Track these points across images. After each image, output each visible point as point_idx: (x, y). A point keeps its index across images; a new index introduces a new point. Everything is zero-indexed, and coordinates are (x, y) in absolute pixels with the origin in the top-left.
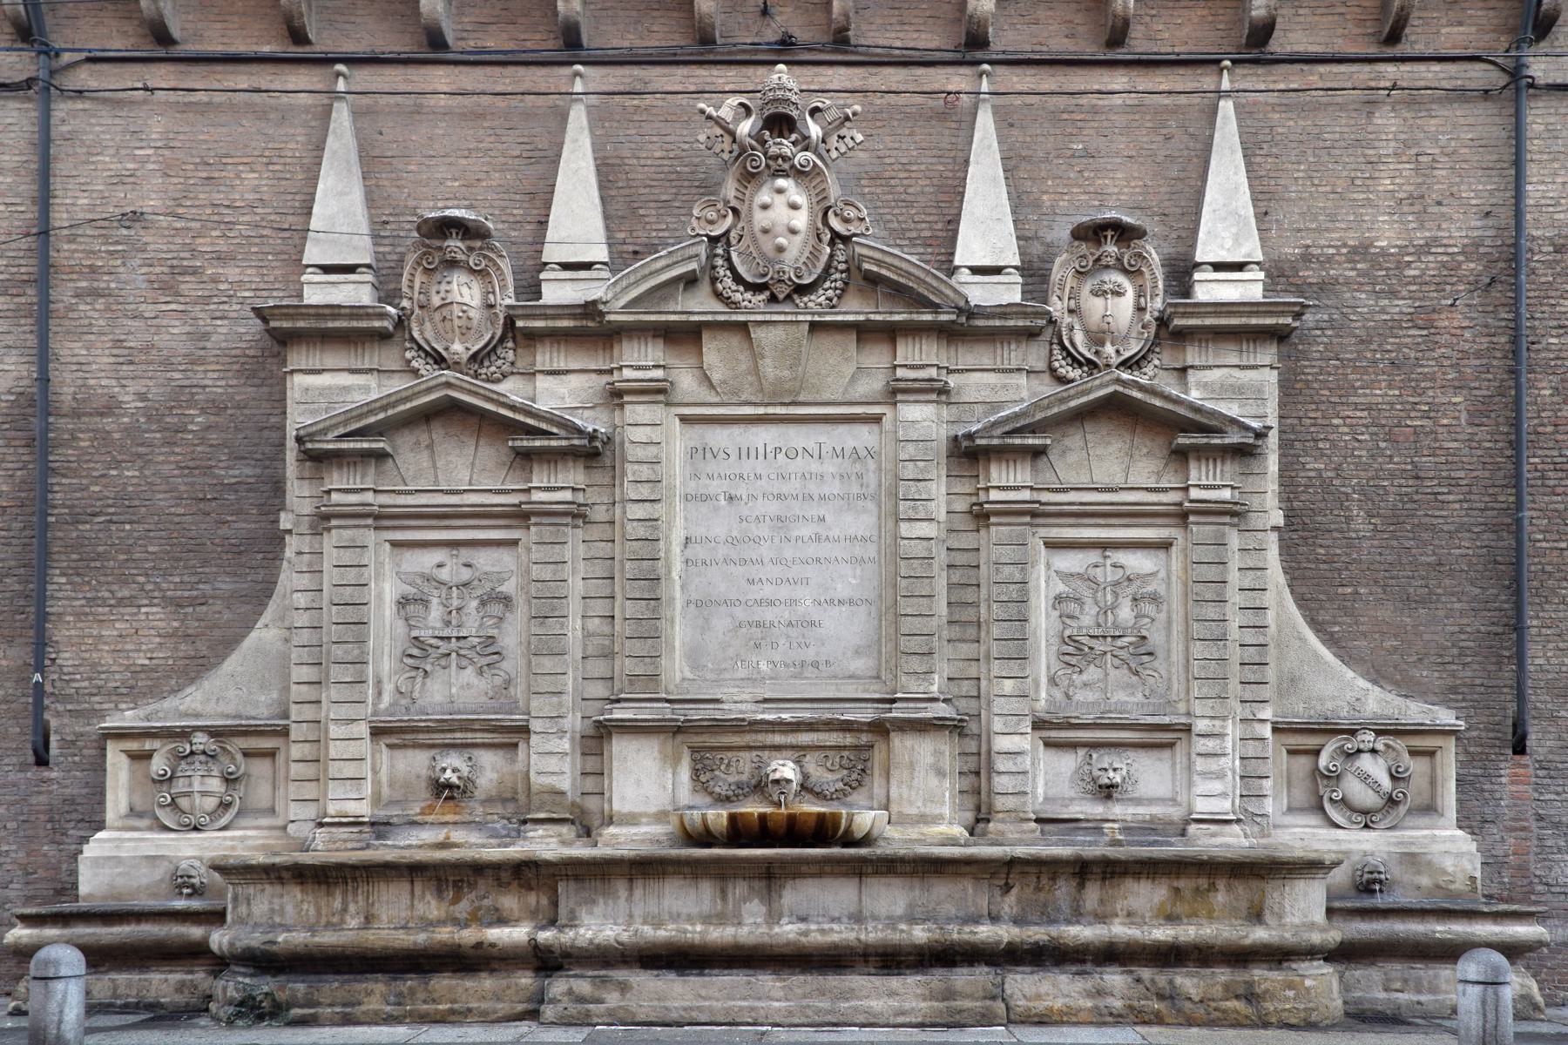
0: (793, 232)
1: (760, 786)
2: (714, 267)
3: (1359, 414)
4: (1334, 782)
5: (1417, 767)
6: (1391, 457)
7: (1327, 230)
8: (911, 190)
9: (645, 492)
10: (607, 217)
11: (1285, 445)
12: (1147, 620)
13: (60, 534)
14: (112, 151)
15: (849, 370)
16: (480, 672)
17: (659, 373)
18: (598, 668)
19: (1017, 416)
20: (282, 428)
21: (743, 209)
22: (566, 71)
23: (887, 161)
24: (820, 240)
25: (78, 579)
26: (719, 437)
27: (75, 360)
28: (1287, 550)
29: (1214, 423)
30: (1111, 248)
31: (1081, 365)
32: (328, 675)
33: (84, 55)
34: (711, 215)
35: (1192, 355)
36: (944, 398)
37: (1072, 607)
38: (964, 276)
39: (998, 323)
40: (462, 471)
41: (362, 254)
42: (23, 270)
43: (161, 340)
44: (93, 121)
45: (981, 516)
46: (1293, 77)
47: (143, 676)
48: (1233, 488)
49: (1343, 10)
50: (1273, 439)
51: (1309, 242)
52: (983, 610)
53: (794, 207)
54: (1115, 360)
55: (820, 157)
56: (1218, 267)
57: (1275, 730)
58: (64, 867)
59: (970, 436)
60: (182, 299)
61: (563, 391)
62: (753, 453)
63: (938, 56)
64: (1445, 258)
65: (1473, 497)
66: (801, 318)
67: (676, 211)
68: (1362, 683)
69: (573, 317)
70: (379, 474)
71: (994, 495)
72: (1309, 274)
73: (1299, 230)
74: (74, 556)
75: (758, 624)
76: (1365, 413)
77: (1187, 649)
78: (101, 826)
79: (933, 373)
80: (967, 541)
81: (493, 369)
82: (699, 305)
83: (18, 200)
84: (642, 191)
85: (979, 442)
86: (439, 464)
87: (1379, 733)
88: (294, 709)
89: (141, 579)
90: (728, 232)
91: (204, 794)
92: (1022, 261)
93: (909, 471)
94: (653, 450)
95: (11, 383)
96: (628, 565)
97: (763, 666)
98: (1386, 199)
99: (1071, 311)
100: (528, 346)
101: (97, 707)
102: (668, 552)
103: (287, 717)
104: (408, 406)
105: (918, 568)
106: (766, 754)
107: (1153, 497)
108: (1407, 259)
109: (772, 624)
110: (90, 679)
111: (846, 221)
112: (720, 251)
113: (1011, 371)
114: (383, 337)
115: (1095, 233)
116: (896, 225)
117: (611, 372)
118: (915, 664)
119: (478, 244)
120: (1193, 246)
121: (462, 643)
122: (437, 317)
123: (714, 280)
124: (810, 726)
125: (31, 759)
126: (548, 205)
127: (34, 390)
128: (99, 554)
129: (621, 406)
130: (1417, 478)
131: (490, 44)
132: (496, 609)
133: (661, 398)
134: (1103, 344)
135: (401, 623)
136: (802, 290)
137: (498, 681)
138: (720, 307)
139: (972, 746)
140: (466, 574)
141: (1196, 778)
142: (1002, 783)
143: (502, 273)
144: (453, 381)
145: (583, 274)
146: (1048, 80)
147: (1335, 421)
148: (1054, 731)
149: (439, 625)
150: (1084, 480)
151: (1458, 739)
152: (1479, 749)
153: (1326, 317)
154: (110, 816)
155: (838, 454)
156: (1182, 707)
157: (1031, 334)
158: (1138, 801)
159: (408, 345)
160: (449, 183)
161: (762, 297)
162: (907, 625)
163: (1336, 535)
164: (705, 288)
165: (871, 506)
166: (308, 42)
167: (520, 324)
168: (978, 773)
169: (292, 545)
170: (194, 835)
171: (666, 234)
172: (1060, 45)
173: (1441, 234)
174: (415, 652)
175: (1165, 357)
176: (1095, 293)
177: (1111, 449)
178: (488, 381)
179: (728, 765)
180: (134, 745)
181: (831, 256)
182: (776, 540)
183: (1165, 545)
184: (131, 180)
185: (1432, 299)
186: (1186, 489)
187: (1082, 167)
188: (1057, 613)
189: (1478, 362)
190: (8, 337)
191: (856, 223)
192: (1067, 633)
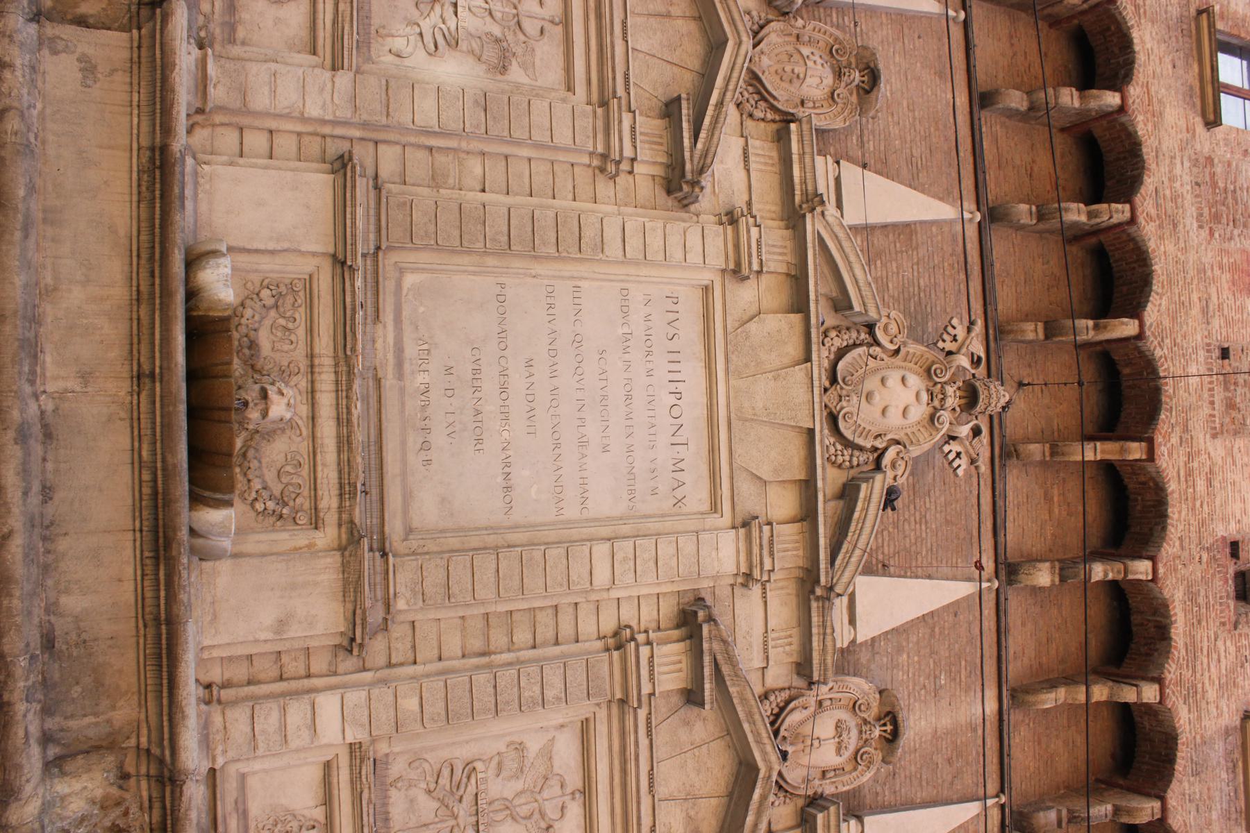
0: (884, 412)
8: (907, 527)
9: (634, 243)
17: (755, 267)
21: (897, 361)
22: (973, 207)
24: (876, 437)
26: (690, 329)
30: (877, 732)
34: (893, 328)
36: (740, 580)
37: (511, 765)
53: (905, 412)
59: (710, 619)
63: (1001, 539)
66: (817, 418)
71: (645, 651)
75: (476, 371)
79: (767, 566)
80: (588, 627)
84: (894, 265)
86: (652, 19)
90: (878, 344)
93: (666, 549)
94: (679, 255)
97: (421, 378)
99: (820, 703)
106: (304, 384)
109: (477, 389)
111: (893, 465)
113: (766, 651)
115: (888, 713)
118: (434, 576)
119: (854, 99)
122: (790, 48)
123: (837, 328)
124: (345, 443)
132: (491, 53)
133: (732, 266)
136: (833, 419)
137: (399, 43)
139: (319, 664)
140: (531, 27)
142: (268, 718)
162: (486, 564)
165: (621, 509)
167: (793, 126)
168: (281, 679)
176: (838, 726)
179: (286, 329)
181: (861, 449)
188: (503, 749)
192: (479, 766)
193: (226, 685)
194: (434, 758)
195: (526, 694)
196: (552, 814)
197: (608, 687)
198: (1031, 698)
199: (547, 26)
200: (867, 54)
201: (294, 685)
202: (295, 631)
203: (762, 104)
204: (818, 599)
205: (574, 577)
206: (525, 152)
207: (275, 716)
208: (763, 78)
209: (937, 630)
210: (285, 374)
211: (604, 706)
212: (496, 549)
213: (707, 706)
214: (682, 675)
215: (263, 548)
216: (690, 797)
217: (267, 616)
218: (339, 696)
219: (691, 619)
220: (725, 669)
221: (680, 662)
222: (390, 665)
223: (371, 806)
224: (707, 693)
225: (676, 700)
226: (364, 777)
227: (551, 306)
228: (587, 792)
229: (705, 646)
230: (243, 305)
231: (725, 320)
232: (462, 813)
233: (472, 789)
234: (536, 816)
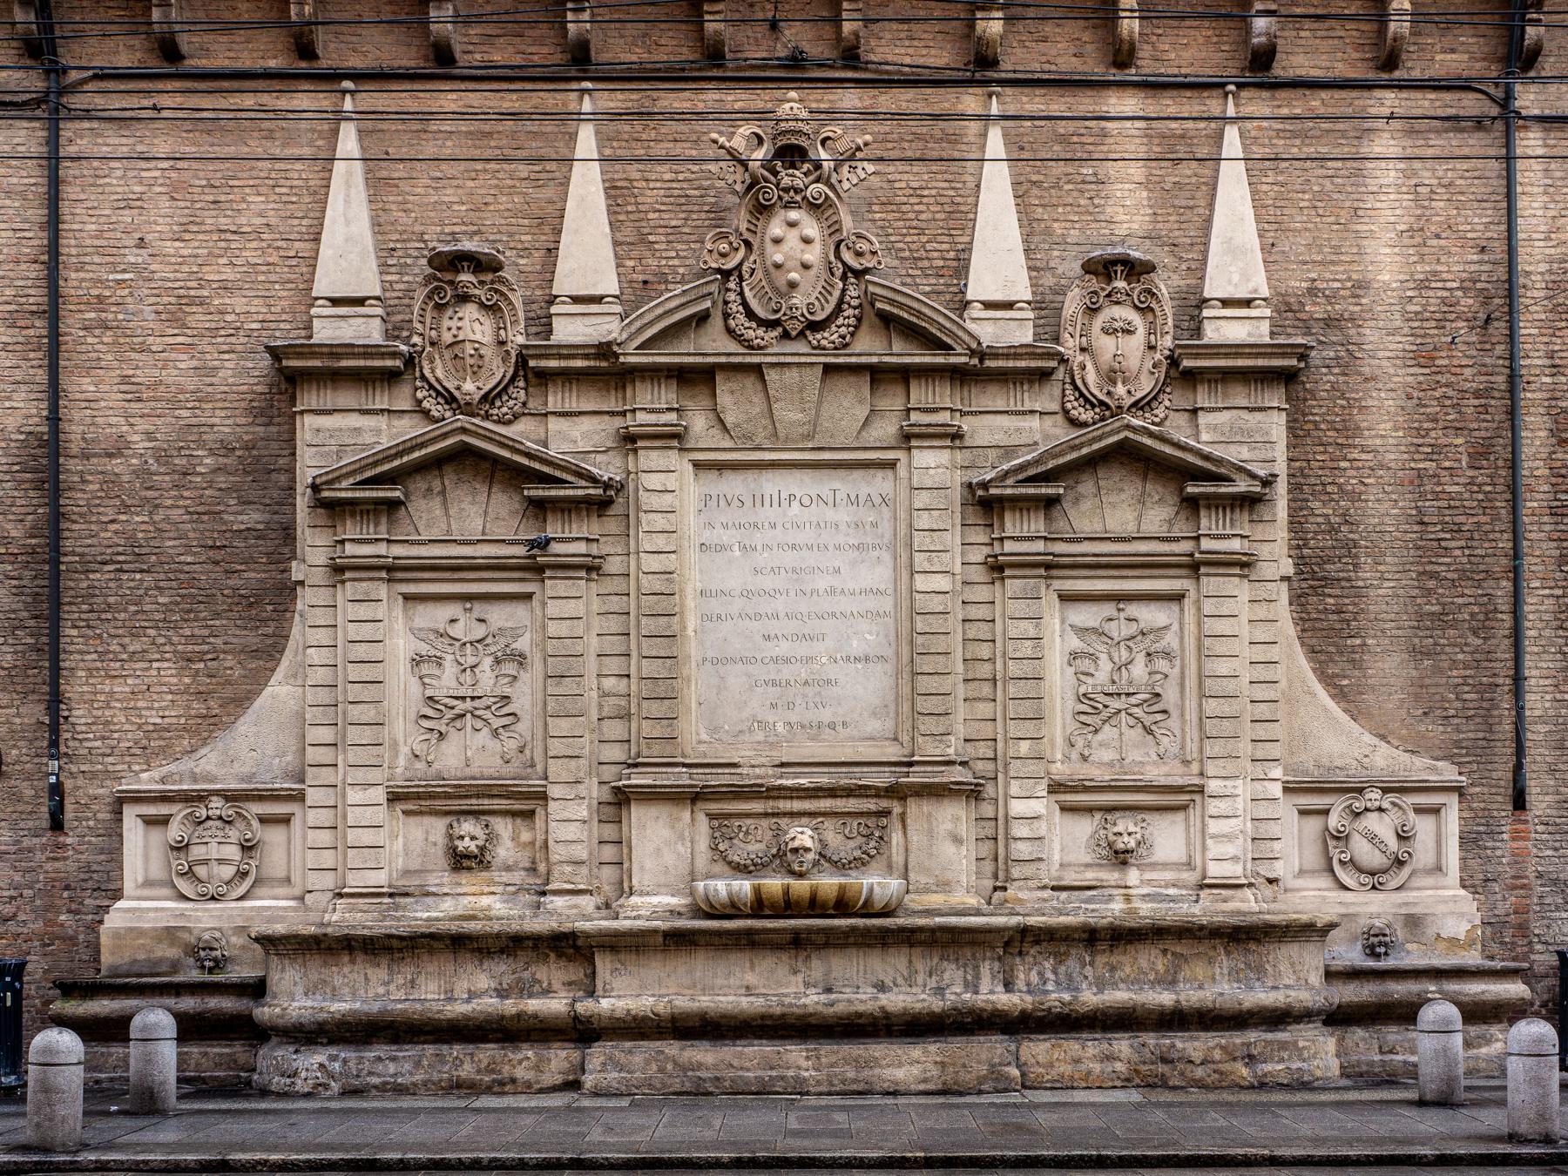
1: (783, 858)
2: (726, 303)
3: (1364, 456)
5: (1424, 827)
7: (1333, 263)
8: (923, 217)
9: (660, 542)
10: (616, 243)
11: (1295, 488)
12: (1159, 676)
13: (72, 584)
14: (119, 173)
15: (862, 412)
16: (495, 733)
17: (672, 417)
18: (615, 729)
19: (1028, 465)
20: (291, 471)
23: (897, 185)
25: (90, 632)
26: (734, 484)
27: (83, 396)
28: (1297, 599)
29: (1223, 470)
30: (1120, 284)
31: (1093, 406)
32: (344, 736)
33: (90, 73)
35: (1203, 398)
36: (957, 442)
37: (1085, 665)
38: (976, 311)
39: (1011, 364)
40: (473, 519)
41: (370, 285)
42: (31, 300)
43: (169, 376)
44: (100, 141)
45: (997, 569)
46: (1296, 103)
47: (155, 735)
48: (1242, 537)
49: (1342, 33)
50: (1281, 487)
51: (1313, 275)
52: (999, 665)
53: (807, 241)
54: (1128, 401)
55: (832, 187)
56: (1226, 303)
57: (1286, 790)
58: (81, 937)
59: (985, 485)
60: (189, 332)
61: (576, 434)
62: (767, 502)
64: (1446, 294)
65: (1475, 544)
67: (685, 237)
68: (1368, 738)
69: (586, 357)
70: (391, 522)
71: (1009, 547)
72: (1316, 310)
73: (1305, 263)
74: (85, 607)
76: (1369, 457)
77: (1200, 705)
78: (117, 895)
79: (944, 417)
81: (505, 410)
82: (713, 344)
83: (26, 226)
84: (651, 216)
85: (993, 491)
87: (1385, 791)
88: (310, 771)
89: (152, 632)
91: (221, 861)
92: (1034, 293)
93: (923, 521)
94: (668, 497)
95: (21, 421)
96: (644, 621)
97: (780, 728)
98: (1388, 231)
99: (1083, 350)
100: (540, 385)
101: (110, 768)
102: (682, 605)
103: (303, 781)
104: (423, 452)
105: (936, 624)
106: (783, 822)
108: (1409, 293)
110: (103, 738)
111: (859, 254)
112: (732, 285)
113: (1024, 413)
114: (390, 378)
115: (1105, 267)
116: (907, 254)
117: (623, 414)
119: (489, 277)
120: (1202, 278)
121: (477, 703)
122: (448, 355)
123: (726, 316)
124: (832, 792)
125: (46, 824)
126: (558, 232)
127: (45, 429)
128: (109, 605)
129: (635, 451)
130: (1422, 523)
131: (497, 57)
132: (509, 668)
134: (1115, 383)
135: (414, 683)
136: (815, 327)
137: (512, 745)
138: (733, 347)
139: (987, 810)
140: (479, 631)
141: (1209, 842)
143: (514, 308)
144: (468, 426)
145: (594, 308)
146: (1057, 103)
147: (1343, 464)
148: (1070, 795)
149: (454, 684)
151: (1461, 795)
152: (1482, 805)
153: (1332, 354)
154: (128, 886)
155: (854, 501)
156: (1195, 768)
157: (1044, 375)
158: (1154, 866)
159: (418, 384)
160: (456, 207)
161: (775, 333)
162: (924, 684)
164: (717, 321)
165: (887, 557)
166: (315, 57)
167: (532, 363)
168: (996, 839)
169: (305, 598)
170: (212, 905)
171: (676, 262)
172: (1066, 63)
173: (1439, 268)
174: (430, 713)
175: (1176, 398)
176: (1105, 331)
177: (1123, 496)
178: (499, 422)
180: (151, 810)
181: (844, 290)
182: (792, 594)
183: (1178, 597)
184: (139, 203)
185: (1432, 336)
186: (1197, 538)
187: (1092, 194)
188: (1072, 670)
189: (1476, 402)
190: (17, 371)
191: (868, 256)
192: (1082, 690)
193: (996, 877)
194: (1072, 726)
195: (1029, 653)
196: (1133, 629)
198: (1126, 47)
199: (475, 614)
200: (436, 262)
201: (1001, 831)
202: (963, 830)
203: (511, 389)
204: (981, 361)
205: (940, 609)
206: (595, 640)
207: (1021, 846)
208: (487, 388)
209: (1034, 178)
210: (778, 832)
212: (914, 674)
213: (1061, 491)
215: (902, 850)
217: (949, 849)
219: (986, 505)
220: (1032, 472)
222: (995, 759)
224: (1050, 491)
225: (1056, 512)
227: (719, 617)
229: (1009, 491)
230: (730, 863)
231: (724, 450)
233: (1101, 698)
234: (1130, 643)
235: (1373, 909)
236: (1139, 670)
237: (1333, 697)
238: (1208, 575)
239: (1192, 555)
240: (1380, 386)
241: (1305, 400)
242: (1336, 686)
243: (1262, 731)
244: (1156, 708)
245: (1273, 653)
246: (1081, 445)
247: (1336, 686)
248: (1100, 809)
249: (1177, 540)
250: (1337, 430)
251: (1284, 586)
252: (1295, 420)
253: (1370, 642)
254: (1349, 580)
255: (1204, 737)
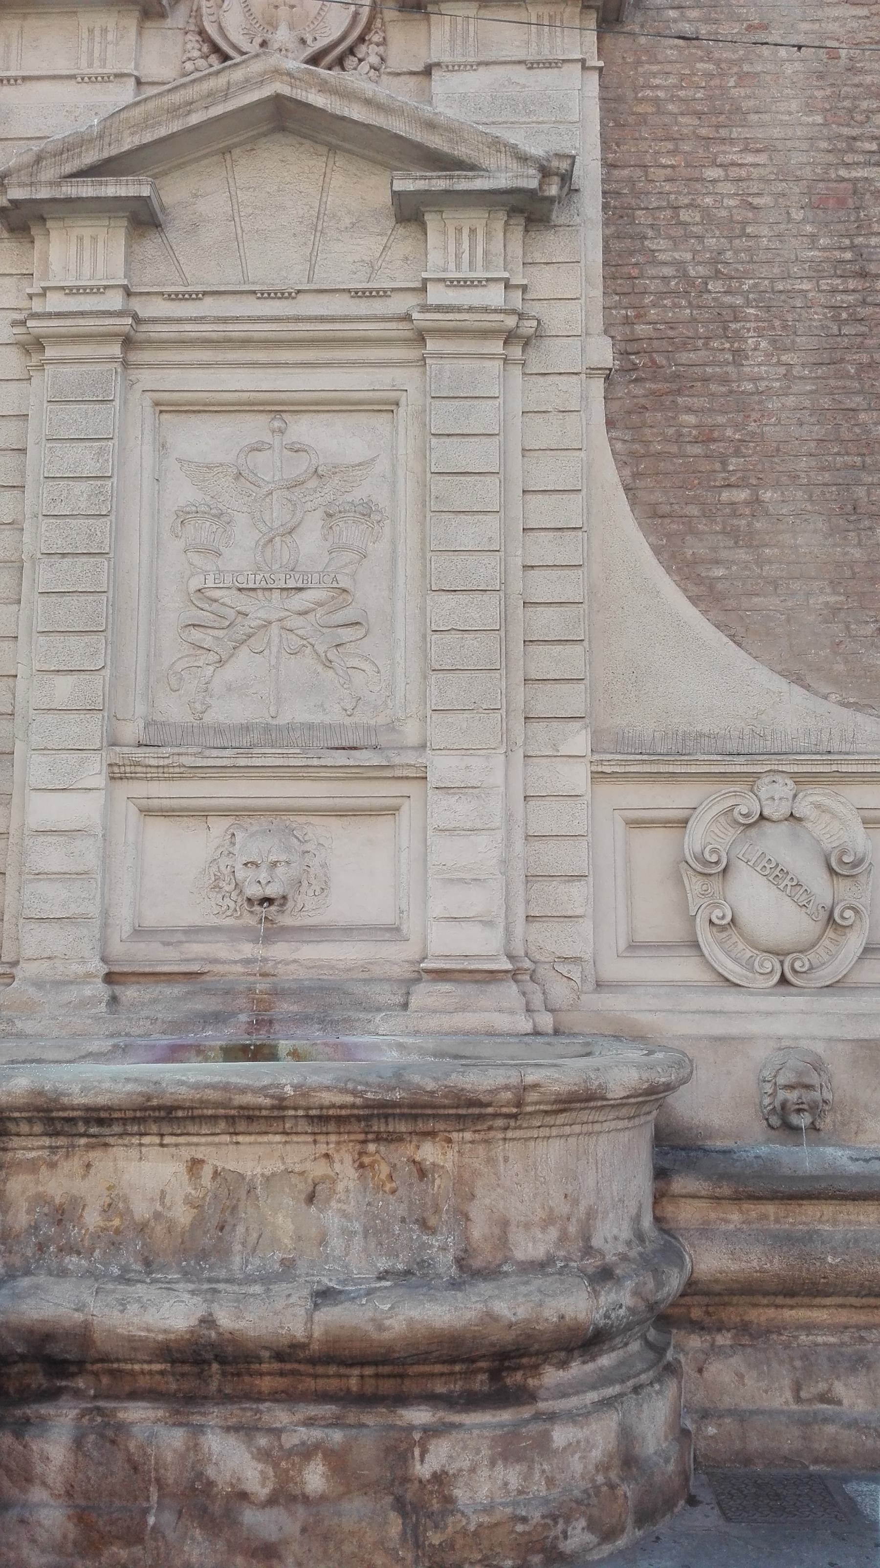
3: (750, 159)
4: (715, 885)
6: (813, 237)
68: (764, 678)
76: (762, 159)
77: (423, 610)
87: (802, 780)
107: (363, 307)
147: (712, 173)
150: (231, 278)
163: (713, 387)
192: (195, 583)
195: (83, 506)
196: (301, 466)
197: (98, 368)
207: (46, 889)
211: (134, 374)
214: (102, 233)
216: (317, 225)
218: (33, 793)
220: (90, 158)
221: (80, 239)
223: (207, 753)
225: (150, 246)
226: (161, 762)
228: (277, 408)
229: (44, 193)
232: (262, 614)
233: (228, 597)
235: (783, 1027)
236: (310, 542)
237: (694, 600)
238: (441, 356)
239: (407, 318)
240: (775, 37)
241: (639, 63)
242: (699, 580)
243: (546, 661)
244: (340, 617)
245: (571, 511)
246: (189, 106)
247: (699, 580)
248: (224, 812)
249: (382, 294)
250: (699, 115)
251: (598, 386)
252: (619, 99)
253: (767, 495)
254: (725, 380)
255: (429, 670)
